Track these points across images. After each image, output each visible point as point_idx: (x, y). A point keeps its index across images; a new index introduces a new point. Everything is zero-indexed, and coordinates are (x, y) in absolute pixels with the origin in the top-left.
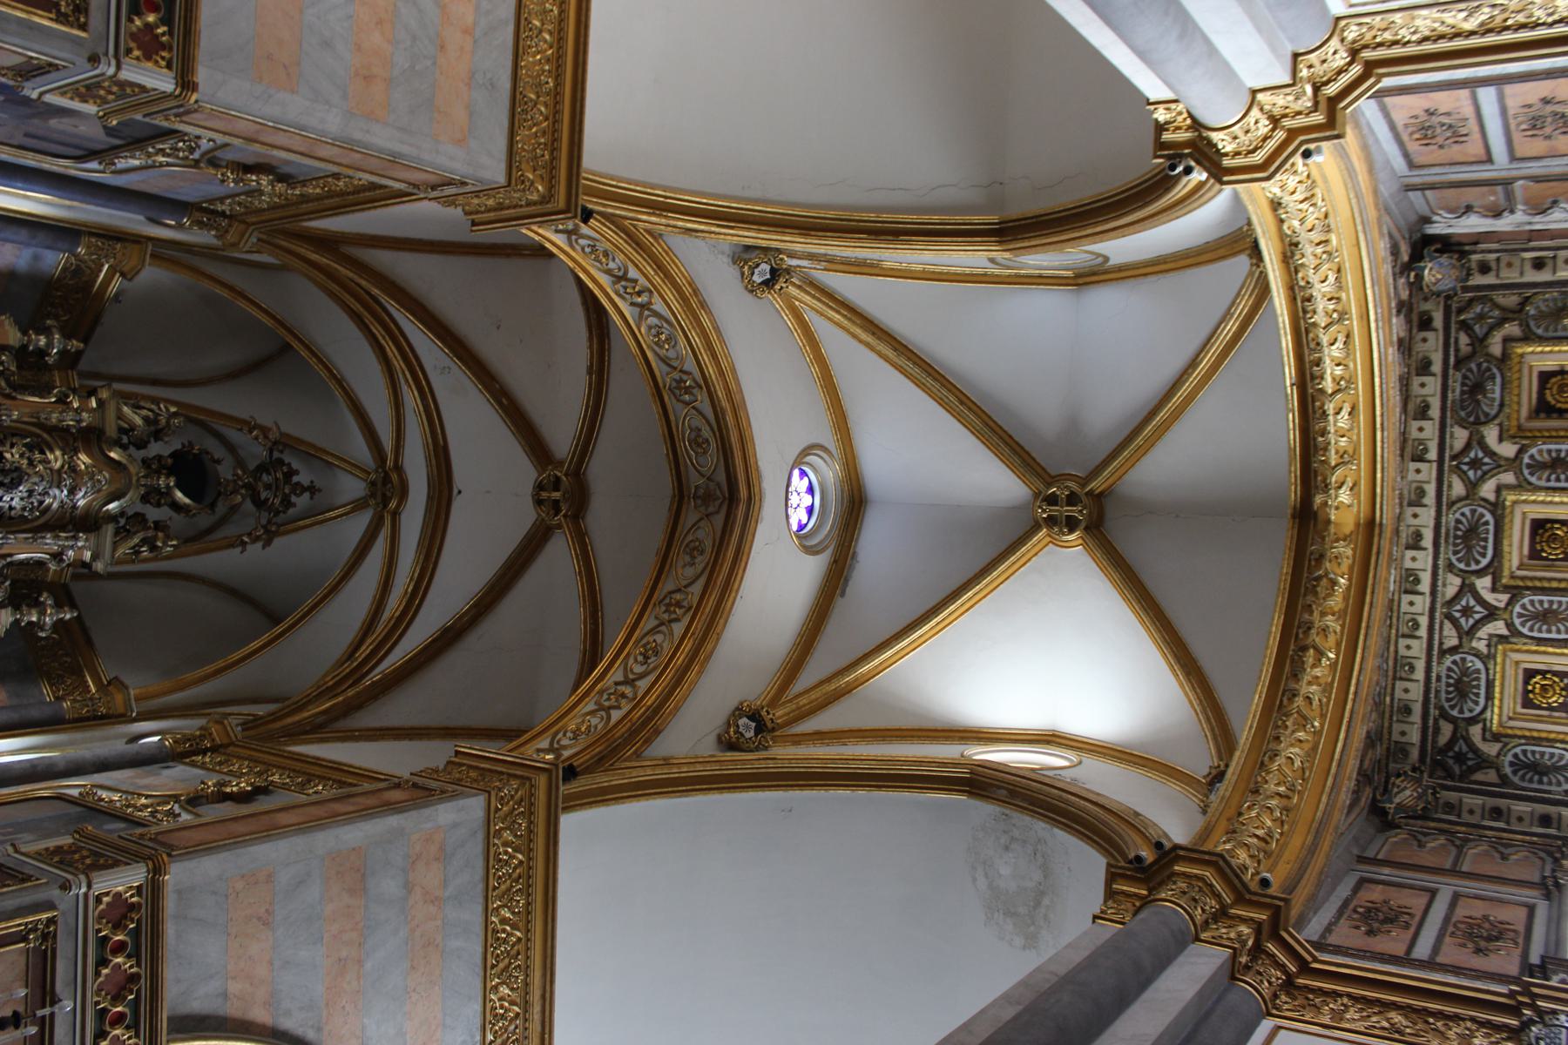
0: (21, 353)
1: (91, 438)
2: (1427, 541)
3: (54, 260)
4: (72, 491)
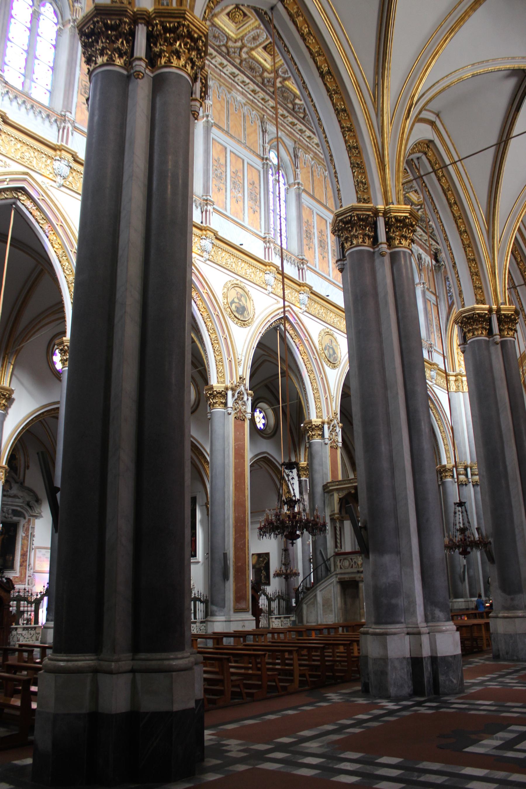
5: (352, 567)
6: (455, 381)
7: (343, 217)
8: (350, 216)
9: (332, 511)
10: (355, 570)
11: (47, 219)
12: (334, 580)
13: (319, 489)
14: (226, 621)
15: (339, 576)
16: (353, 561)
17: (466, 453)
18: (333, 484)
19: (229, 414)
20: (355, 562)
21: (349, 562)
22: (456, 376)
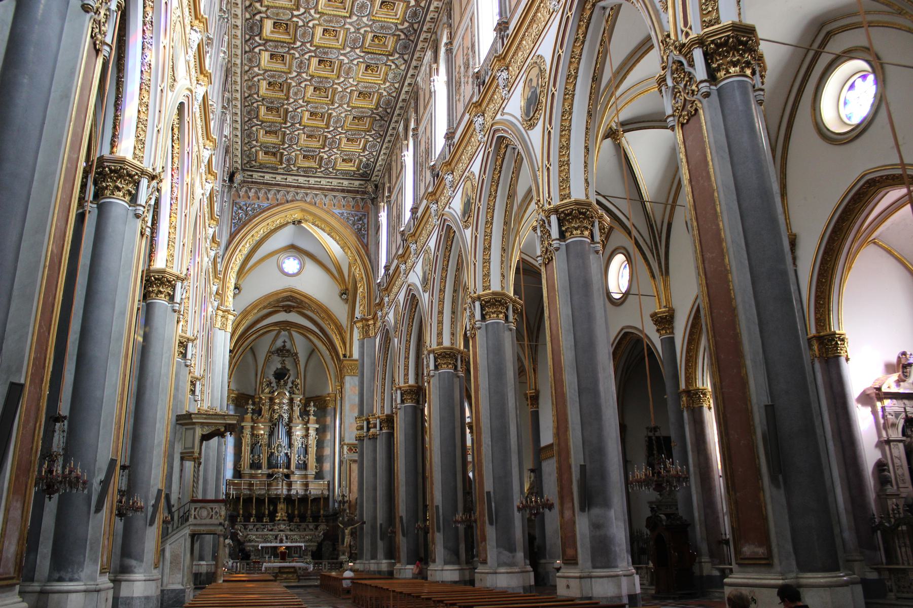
1: (272, 400)
2: (308, 179)
4: (284, 404)
5: (211, 518)
7: (580, 207)
8: (586, 209)
9: (185, 448)
10: (217, 522)
12: (187, 531)
15: (191, 528)
16: (214, 511)
18: (197, 416)
20: (216, 512)
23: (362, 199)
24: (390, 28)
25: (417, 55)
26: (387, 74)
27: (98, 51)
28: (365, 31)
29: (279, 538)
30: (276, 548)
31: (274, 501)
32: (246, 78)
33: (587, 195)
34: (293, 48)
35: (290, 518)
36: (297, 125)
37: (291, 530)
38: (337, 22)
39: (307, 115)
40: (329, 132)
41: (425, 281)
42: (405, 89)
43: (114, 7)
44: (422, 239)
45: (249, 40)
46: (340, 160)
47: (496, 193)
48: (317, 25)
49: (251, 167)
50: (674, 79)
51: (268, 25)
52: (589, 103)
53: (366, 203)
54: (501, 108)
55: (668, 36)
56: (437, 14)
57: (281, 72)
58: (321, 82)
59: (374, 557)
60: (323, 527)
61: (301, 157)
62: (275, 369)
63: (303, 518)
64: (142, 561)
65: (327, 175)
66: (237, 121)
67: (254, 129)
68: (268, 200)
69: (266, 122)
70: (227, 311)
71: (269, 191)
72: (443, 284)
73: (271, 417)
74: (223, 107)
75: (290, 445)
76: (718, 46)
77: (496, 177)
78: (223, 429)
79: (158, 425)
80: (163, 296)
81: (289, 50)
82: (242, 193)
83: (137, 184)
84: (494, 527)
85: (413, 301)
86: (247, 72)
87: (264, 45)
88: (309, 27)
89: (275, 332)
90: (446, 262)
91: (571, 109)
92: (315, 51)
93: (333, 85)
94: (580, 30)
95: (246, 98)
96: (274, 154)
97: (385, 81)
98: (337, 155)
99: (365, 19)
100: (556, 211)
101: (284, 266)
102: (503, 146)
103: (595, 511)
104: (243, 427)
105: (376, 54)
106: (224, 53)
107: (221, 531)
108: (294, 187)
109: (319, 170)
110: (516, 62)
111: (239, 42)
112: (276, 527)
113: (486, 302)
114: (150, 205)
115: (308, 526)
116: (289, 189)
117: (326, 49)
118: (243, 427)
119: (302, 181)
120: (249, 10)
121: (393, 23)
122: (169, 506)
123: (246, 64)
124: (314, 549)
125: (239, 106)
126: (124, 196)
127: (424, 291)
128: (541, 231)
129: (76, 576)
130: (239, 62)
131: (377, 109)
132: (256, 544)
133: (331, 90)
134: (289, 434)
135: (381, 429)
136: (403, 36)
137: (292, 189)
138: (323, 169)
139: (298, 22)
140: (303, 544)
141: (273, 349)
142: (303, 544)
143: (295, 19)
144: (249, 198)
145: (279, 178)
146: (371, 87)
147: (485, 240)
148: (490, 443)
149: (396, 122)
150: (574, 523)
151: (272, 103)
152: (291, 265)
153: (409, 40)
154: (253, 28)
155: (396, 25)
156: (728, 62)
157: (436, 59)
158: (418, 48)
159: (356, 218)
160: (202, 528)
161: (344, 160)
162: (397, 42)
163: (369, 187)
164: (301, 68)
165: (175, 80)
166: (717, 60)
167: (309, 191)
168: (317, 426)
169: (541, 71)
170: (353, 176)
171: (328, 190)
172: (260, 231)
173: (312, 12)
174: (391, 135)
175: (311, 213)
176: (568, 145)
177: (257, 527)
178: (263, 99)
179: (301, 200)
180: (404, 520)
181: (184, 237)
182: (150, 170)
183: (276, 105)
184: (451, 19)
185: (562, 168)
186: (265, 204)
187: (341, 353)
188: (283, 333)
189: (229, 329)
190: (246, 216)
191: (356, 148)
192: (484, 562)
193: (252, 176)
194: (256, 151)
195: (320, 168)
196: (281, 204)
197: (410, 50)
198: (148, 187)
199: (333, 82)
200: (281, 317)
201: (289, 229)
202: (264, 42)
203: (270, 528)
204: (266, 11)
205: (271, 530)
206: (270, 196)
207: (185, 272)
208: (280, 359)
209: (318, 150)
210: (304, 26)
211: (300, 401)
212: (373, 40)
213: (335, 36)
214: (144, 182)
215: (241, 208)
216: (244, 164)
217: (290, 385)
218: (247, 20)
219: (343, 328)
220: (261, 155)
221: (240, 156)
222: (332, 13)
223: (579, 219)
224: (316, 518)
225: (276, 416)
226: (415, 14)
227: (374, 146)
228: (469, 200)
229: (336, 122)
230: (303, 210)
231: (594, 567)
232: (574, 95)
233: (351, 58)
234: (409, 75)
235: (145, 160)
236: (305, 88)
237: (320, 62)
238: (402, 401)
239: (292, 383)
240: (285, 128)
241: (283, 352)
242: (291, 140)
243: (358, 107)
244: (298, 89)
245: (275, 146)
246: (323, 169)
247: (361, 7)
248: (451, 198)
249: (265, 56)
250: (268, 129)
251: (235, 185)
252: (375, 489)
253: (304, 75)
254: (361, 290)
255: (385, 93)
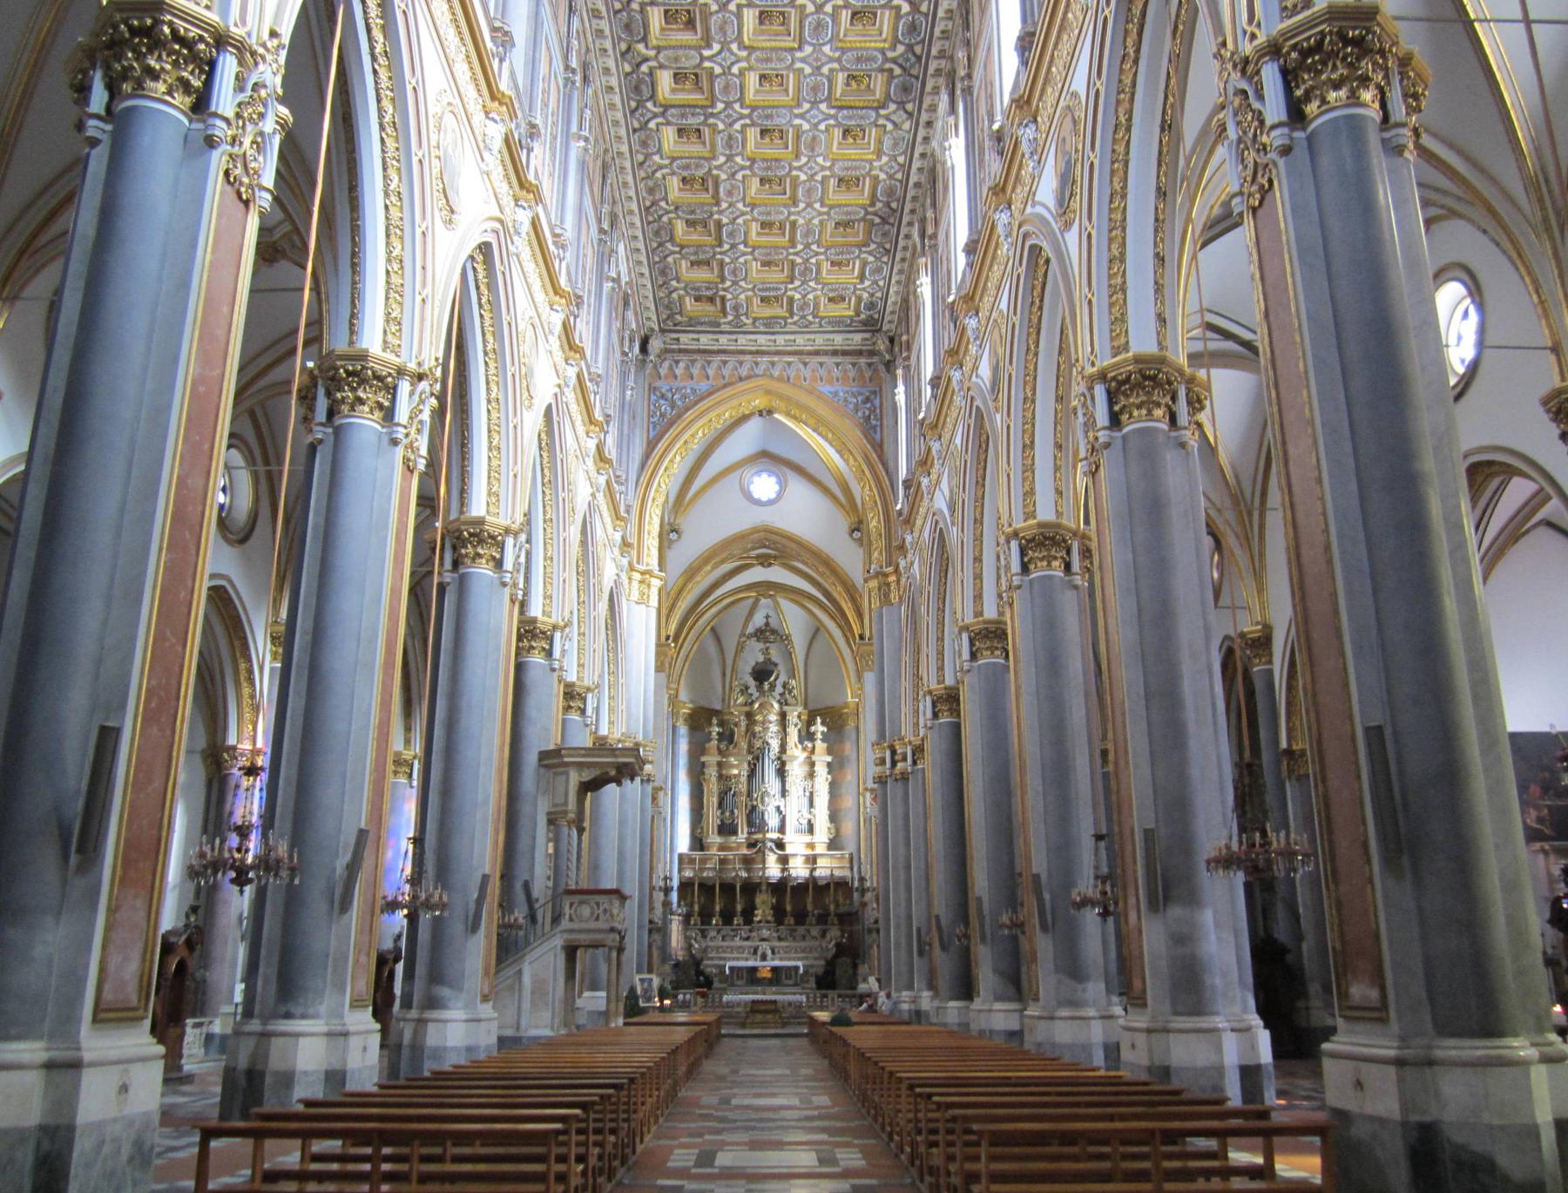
0: (720, 740)
1: (750, 716)
2: (773, 337)
3: (683, 730)
5: (597, 919)
6: (640, 582)
7: (1145, 366)
9: (555, 805)
10: (606, 926)
11: (393, 56)
12: (558, 942)
13: (530, 759)
14: (467, 1021)
15: (566, 936)
17: (638, 720)
19: (504, 585)
20: (605, 911)
21: (592, 908)
22: (643, 573)
23: (870, 365)
24: (874, 59)
25: (927, 101)
26: (880, 142)
27: (246, 203)
28: (831, 70)
29: (759, 953)
30: (754, 970)
31: (751, 888)
32: (643, 174)
33: (1159, 343)
34: (712, 115)
35: (779, 914)
36: (741, 247)
37: (780, 939)
38: (781, 60)
39: (755, 227)
40: (796, 254)
41: (952, 510)
42: (916, 164)
43: (269, 125)
44: (946, 436)
45: (636, 109)
46: (823, 301)
47: (1037, 346)
48: (746, 69)
49: (675, 325)
50: (1239, 123)
51: (665, 80)
52: (1159, 172)
53: (876, 370)
54: (1031, 193)
55: (1224, 44)
56: (950, 23)
57: (700, 158)
58: (768, 168)
59: (910, 987)
60: (834, 932)
61: (757, 301)
62: (753, 664)
63: (801, 918)
64: (461, 989)
65: (805, 328)
66: (638, 250)
67: (670, 259)
68: (708, 378)
69: (688, 246)
70: (649, 572)
71: (709, 363)
72: (979, 509)
73: (750, 746)
74: (602, 231)
75: (784, 793)
76: (1305, 53)
77: (1035, 320)
78: (613, 773)
79: (483, 770)
80: (484, 561)
81: (706, 119)
82: (663, 371)
83: (393, 391)
84: (1050, 935)
85: (941, 539)
86: (641, 164)
87: (663, 114)
88: (734, 75)
89: (751, 601)
90: (981, 472)
91: (1124, 187)
92: (749, 116)
93: (790, 171)
94: (1129, 40)
95: (647, 209)
96: (711, 300)
97: (879, 153)
98: (815, 291)
99: (826, 49)
100: (1102, 376)
101: (752, 488)
102: (1042, 262)
103: (1175, 912)
104: (703, 764)
105: (856, 108)
106: (586, 140)
107: (613, 940)
108: (751, 353)
109: (790, 321)
110: (1045, 109)
111: (619, 115)
112: (754, 934)
113: (1028, 541)
114: (421, 422)
115: (809, 931)
116: (742, 358)
117: (769, 110)
118: (703, 763)
119: (763, 342)
120: (629, 56)
121: (876, 49)
122: (530, 901)
123: (637, 152)
124: (820, 971)
125: (638, 224)
126: (371, 412)
127: (953, 524)
128: (1084, 415)
129: (311, 1011)
130: (625, 148)
131: (872, 204)
132: (722, 962)
133: (788, 180)
134: (782, 773)
135: (915, 763)
136: (897, 71)
137: (748, 357)
138: (796, 318)
139: (712, 68)
140: (800, 964)
141: (750, 630)
142: (800, 964)
143: (707, 64)
144: (676, 377)
145: (723, 339)
146: (855, 168)
147: (1024, 432)
148: (1040, 788)
149: (910, 224)
150: (1140, 931)
151: (693, 212)
152: (764, 485)
153: (910, 75)
154: (639, 89)
155: (882, 51)
156: (1324, 83)
157: (953, 109)
158: (928, 88)
159: (860, 399)
160: (582, 937)
161: (831, 300)
162: (889, 83)
163: (880, 342)
164: (731, 147)
165: (452, 212)
166: (1304, 82)
167: (776, 359)
168: (829, 759)
169: (1074, 122)
170: (850, 325)
171: (810, 353)
172: (697, 434)
173: (734, 47)
174: (905, 248)
175: (781, 397)
176: (1123, 254)
177: (723, 933)
178: (677, 208)
179: (764, 375)
180: (943, 922)
181: (516, 463)
182: (412, 366)
183: (699, 216)
184: (968, 29)
185: (1114, 298)
186: (704, 386)
187: (857, 630)
188: (763, 601)
189: (654, 601)
190: (673, 408)
191: (848, 277)
192: (1036, 999)
193: (678, 340)
194: (680, 297)
195: (792, 317)
196: (730, 384)
197: (916, 93)
198: (412, 393)
199: (790, 165)
200: (757, 574)
201: (754, 425)
202: (661, 110)
203: (744, 935)
204: (656, 56)
205: (747, 939)
206: (711, 372)
207: (519, 519)
208: (761, 645)
209: (783, 287)
210: (724, 73)
211: (799, 717)
212: (848, 84)
213: (782, 85)
214: (404, 387)
215: (663, 396)
216: (664, 321)
217: (779, 689)
218: (627, 75)
219: (856, 589)
220: (689, 303)
221: (653, 308)
222: (768, 44)
223: (1144, 388)
224: (823, 919)
225: (758, 744)
226: (913, 28)
227: (879, 270)
228: (998, 364)
229: (806, 235)
230: (768, 392)
231: (1176, 1013)
232: (1126, 163)
233: (812, 121)
234: (919, 139)
235: (404, 352)
236: (743, 182)
237: (764, 132)
238: (935, 715)
239: (784, 687)
240: (720, 253)
241: (765, 634)
242: (734, 273)
243: (839, 206)
244: (732, 185)
245: (710, 285)
246: (796, 318)
247: (816, 28)
248: (977, 359)
249: (669, 134)
250: (692, 258)
251: (652, 358)
252: (908, 867)
253: (738, 159)
254: (874, 523)
255: (882, 176)
